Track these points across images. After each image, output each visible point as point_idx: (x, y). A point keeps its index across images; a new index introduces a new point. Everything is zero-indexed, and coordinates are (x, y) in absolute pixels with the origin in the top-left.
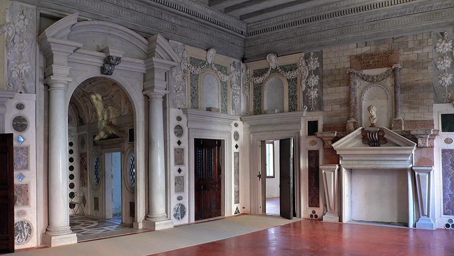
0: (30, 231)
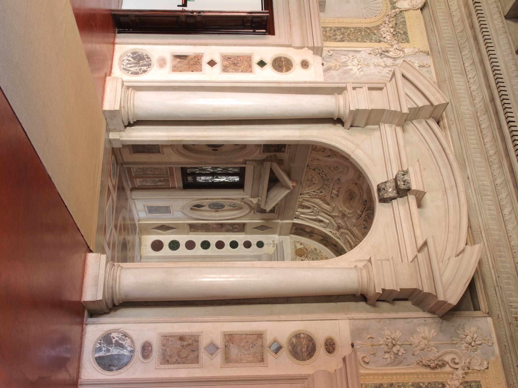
0: (136, 73)
